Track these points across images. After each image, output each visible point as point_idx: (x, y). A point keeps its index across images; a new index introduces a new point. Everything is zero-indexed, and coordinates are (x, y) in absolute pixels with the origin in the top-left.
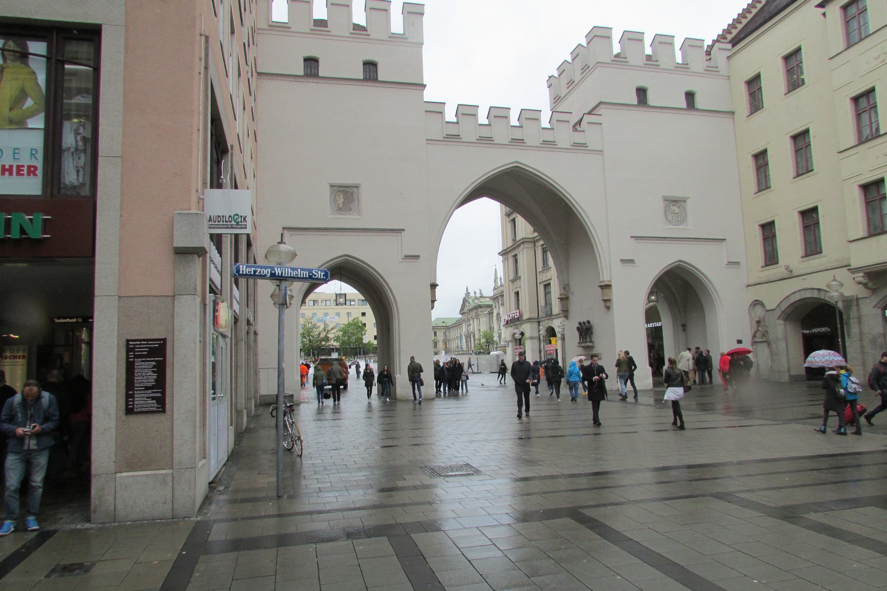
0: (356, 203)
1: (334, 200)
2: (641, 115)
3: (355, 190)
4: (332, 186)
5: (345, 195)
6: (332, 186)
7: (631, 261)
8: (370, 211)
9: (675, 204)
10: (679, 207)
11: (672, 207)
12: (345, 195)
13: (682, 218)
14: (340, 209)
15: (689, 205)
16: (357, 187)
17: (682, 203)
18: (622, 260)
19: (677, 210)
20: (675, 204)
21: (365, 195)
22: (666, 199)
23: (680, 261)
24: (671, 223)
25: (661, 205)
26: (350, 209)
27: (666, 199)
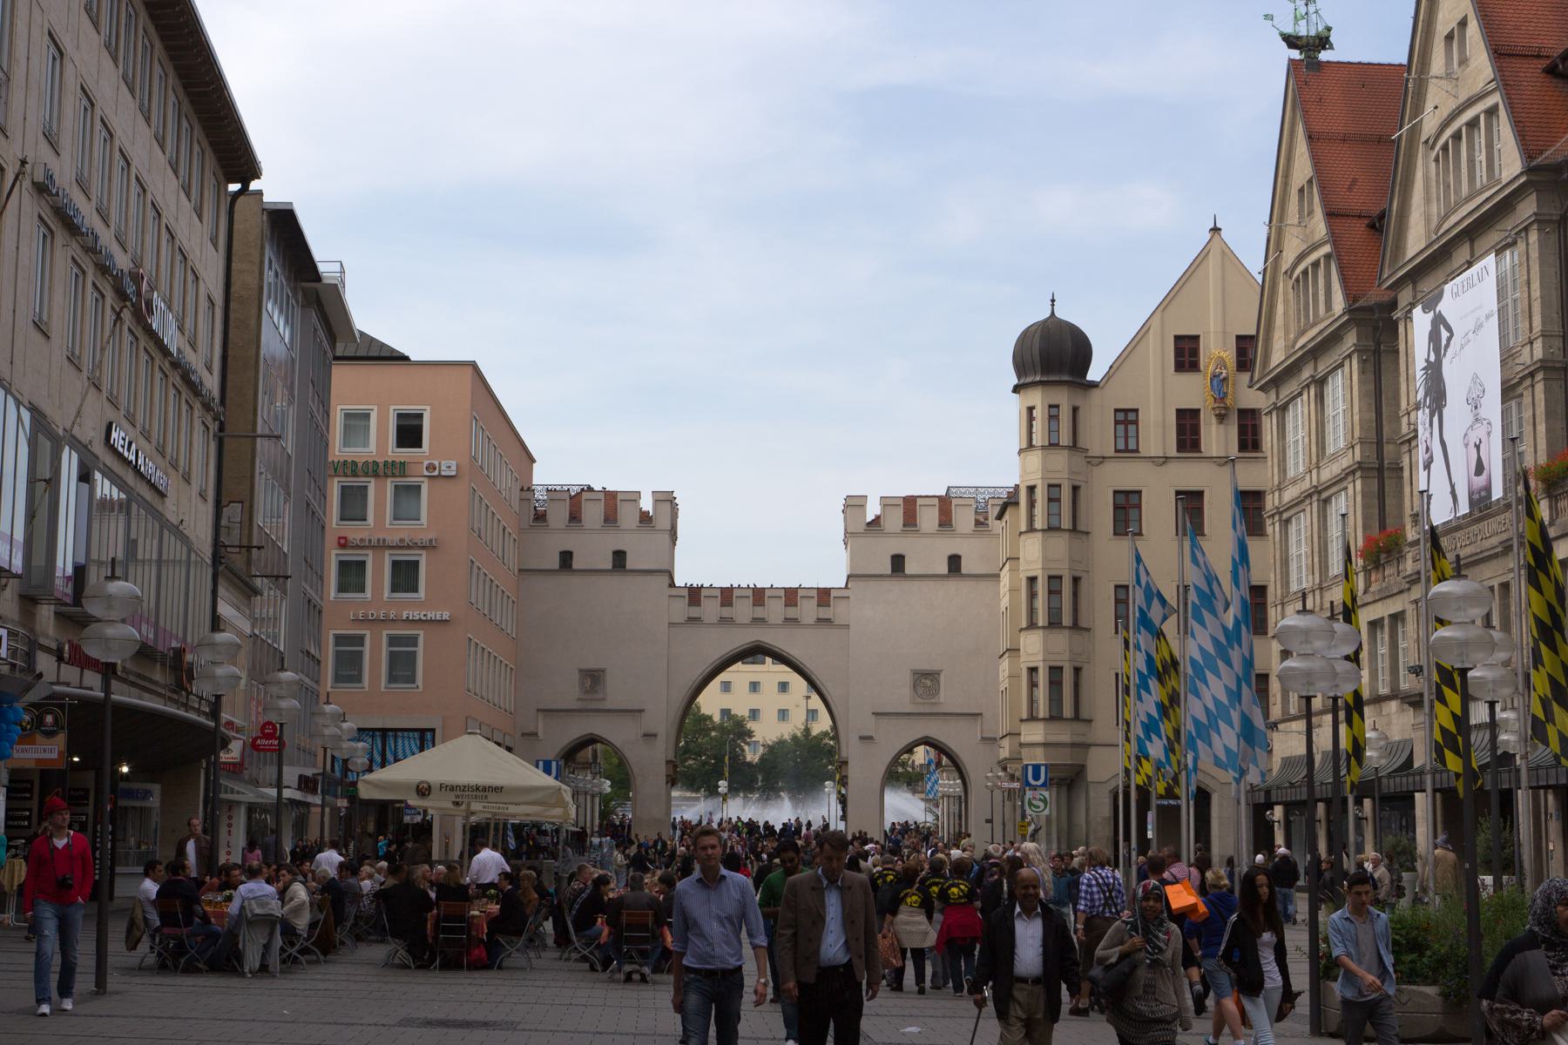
1: (582, 684)
2: (896, 587)
4: (581, 671)
5: (593, 678)
6: (581, 671)
7: (871, 738)
8: (616, 693)
9: (926, 680)
13: (934, 691)
14: (587, 692)
15: (942, 679)
18: (861, 738)
19: (928, 683)
20: (926, 680)
22: (915, 673)
24: (921, 696)
25: (908, 678)
27: (915, 673)
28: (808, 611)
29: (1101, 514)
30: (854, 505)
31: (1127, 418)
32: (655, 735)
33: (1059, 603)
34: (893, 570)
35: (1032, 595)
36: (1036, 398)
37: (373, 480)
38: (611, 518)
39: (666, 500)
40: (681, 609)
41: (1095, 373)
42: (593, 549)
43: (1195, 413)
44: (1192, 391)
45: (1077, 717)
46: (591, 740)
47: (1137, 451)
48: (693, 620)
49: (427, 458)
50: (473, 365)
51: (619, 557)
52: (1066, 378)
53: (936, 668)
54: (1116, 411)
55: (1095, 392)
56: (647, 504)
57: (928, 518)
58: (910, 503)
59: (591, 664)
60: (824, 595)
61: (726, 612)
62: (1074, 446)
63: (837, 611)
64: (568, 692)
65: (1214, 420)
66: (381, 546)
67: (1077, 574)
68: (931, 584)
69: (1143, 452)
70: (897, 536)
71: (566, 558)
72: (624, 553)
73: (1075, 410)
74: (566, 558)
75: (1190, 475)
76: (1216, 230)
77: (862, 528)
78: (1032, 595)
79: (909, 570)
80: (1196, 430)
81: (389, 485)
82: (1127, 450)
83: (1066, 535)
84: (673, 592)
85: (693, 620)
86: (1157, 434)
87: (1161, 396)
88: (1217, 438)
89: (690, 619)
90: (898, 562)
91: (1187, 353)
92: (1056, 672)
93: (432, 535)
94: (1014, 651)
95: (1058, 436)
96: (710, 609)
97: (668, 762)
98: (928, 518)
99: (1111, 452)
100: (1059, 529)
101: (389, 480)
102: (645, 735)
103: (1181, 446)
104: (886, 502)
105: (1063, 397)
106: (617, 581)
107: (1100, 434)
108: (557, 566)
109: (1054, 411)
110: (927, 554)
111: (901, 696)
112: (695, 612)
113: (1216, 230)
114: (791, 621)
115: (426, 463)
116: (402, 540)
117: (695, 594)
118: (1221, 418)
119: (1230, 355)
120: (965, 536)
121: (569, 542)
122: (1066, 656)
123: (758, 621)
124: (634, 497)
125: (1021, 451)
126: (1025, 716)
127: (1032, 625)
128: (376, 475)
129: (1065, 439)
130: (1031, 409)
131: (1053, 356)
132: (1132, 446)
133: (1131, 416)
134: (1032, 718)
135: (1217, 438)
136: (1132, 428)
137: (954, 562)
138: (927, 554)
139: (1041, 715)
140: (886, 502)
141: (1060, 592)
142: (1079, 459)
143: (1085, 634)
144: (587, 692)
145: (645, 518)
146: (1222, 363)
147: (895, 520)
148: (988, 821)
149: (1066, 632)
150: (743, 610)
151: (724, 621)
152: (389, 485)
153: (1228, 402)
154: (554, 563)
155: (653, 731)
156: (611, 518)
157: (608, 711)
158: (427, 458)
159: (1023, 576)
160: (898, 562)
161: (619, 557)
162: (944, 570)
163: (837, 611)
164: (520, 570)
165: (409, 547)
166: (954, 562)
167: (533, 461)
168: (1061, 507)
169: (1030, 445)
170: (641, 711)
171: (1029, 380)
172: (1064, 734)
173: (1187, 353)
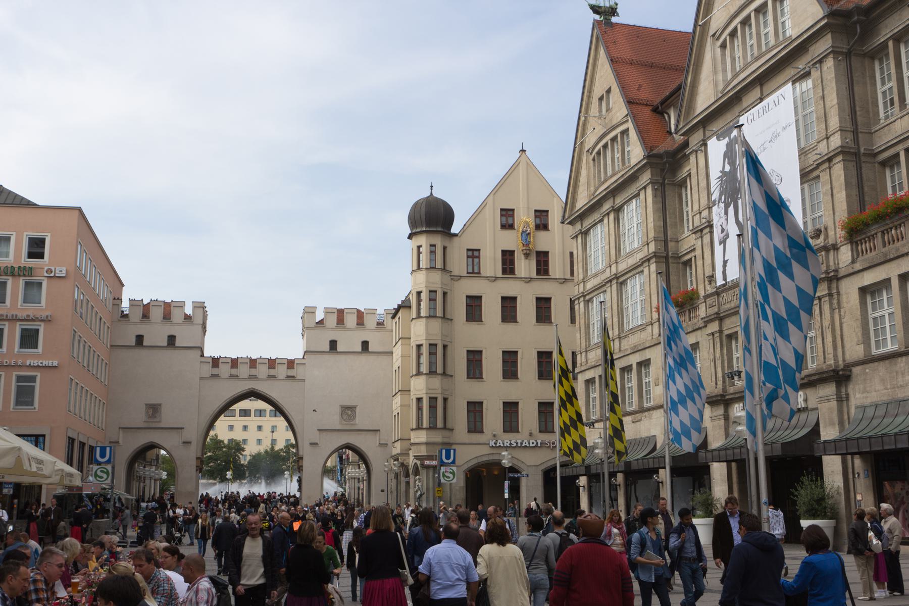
1: (147, 412)
2: (332, 358)
5: (154, 409)
7: (316, 444)
8: (167, 418)
9: (348, 411)
12: (154, 409)
13: (353, 417)
14: (150, 417)
15: (357, 410)
16: (160, 405)
18: (311, 444)
19: (350, 412)
20: (348, 411)
22: (342, 407)
25: (338, 410)
27: (342, 407)
28: (281, 371)
29: (459, 309)
30: (309, 311)
31: (474, 254)
32: (190, 443)
33: (436, 360)
35: (419, 355)
36: (422, 240)
37: (10, 278)
38: (167, 317)
39: (200, 307)
40: (207, 370)
41: (455, 229)
42: (156, 334)
43: (512, 253)
44: (511, 240)
45: (445, 428)
46: (153, 446)
47: (479, 273)
48: (214, 376)
49: (47, 265)
50: (79, 210)
51: (172, 339)
52: (440, 229)
54: (468, 250)
55: (456, 239)
56: (188, 310)
57: (351, 321)
58: (341, 313)
59: (153, 402)
60: (291, 363)
61: (234, 371)
62: (444, 269)
63: (298, 372)
64: (138, 417)
65: (523, 256)
66: (14, 319)
67: (446, 343)
68: (352, 357)
69: (483, 273)
70: (335, 331)
73: (445, 248)
74: (140, 339)
75: (509, 288)
76: (523, 151)
77: (312, 324)
78: (419, 355)
79: (340, 348)
80: (512, 262)
81: (21, 282)
82: (474, 272)
83: (440, 320)
84: (203, 359)
85: (214, 376)
86: (491, 264)
87: (493, 242)
88: (525, 267)
89: (213, 376)
90: (333, 344)
91: (507, 219)
92: (433, 400)
93: (48, 313)
94: (406, 391)
95: (438, 264)
96: (225, 370)
97: (197, 458)
98: (351, 321)
99: (465, 274)
100: (435, 317)
101: (22, 278)
103: (504, 271)
104: (327, 311)
105: (438, 240)
106: (170, 353)
107: (459, 263)
109: (433, 249)
110: (349, 340)
111: (334, 420)
112: (215, 371)
113: (523, 151)
114: (272, 377)
115: (46, 268)
116: (28, 316)
117: (215, 362)
118: (527, 256)
119: (531, 220)
121: (142, 330)
122: (439, 391)
123: (252, 377)
124: (181, 305)
125: (413, 271)
126: (414, 427)
127: (419, 373)
128: (13, 275)
129: (439, 264)
130: (419, 247)
131: (432, 218)
132: (476, 271)
133: (476, 254)
134: (419, 427)
135: (525, 267)
136: (476, 260)
137: (365, 345)
138: (349, 340)
139: (424, 426)
140: (327, 311)
141: (436, 354)
142: (447, 277)
143: (450, 378)
144: (150, 417)
145: (188, 318)
146: (527, 224)
147: (332, 321)
148: (383, 491)
149: (440, 377)
150: (244, 371)
151: (233, 377)
152: (21, 282)
153: (531, 247)
155: (189, 440)
156: (167, 317)
158: (47, 265)
159: (413, 344)
160: (333, 344)
161: (172, 339)
162: (359, 349)
163: (298, 372)
164: (111, 346)
165: (32, 320)
166: (365, 345)
167: (123, 285)
168: (436, 304)
169: (419, 268)
170: (182, 428)
171: (418, 230)
172: (437, 437)
173: (507, 219)
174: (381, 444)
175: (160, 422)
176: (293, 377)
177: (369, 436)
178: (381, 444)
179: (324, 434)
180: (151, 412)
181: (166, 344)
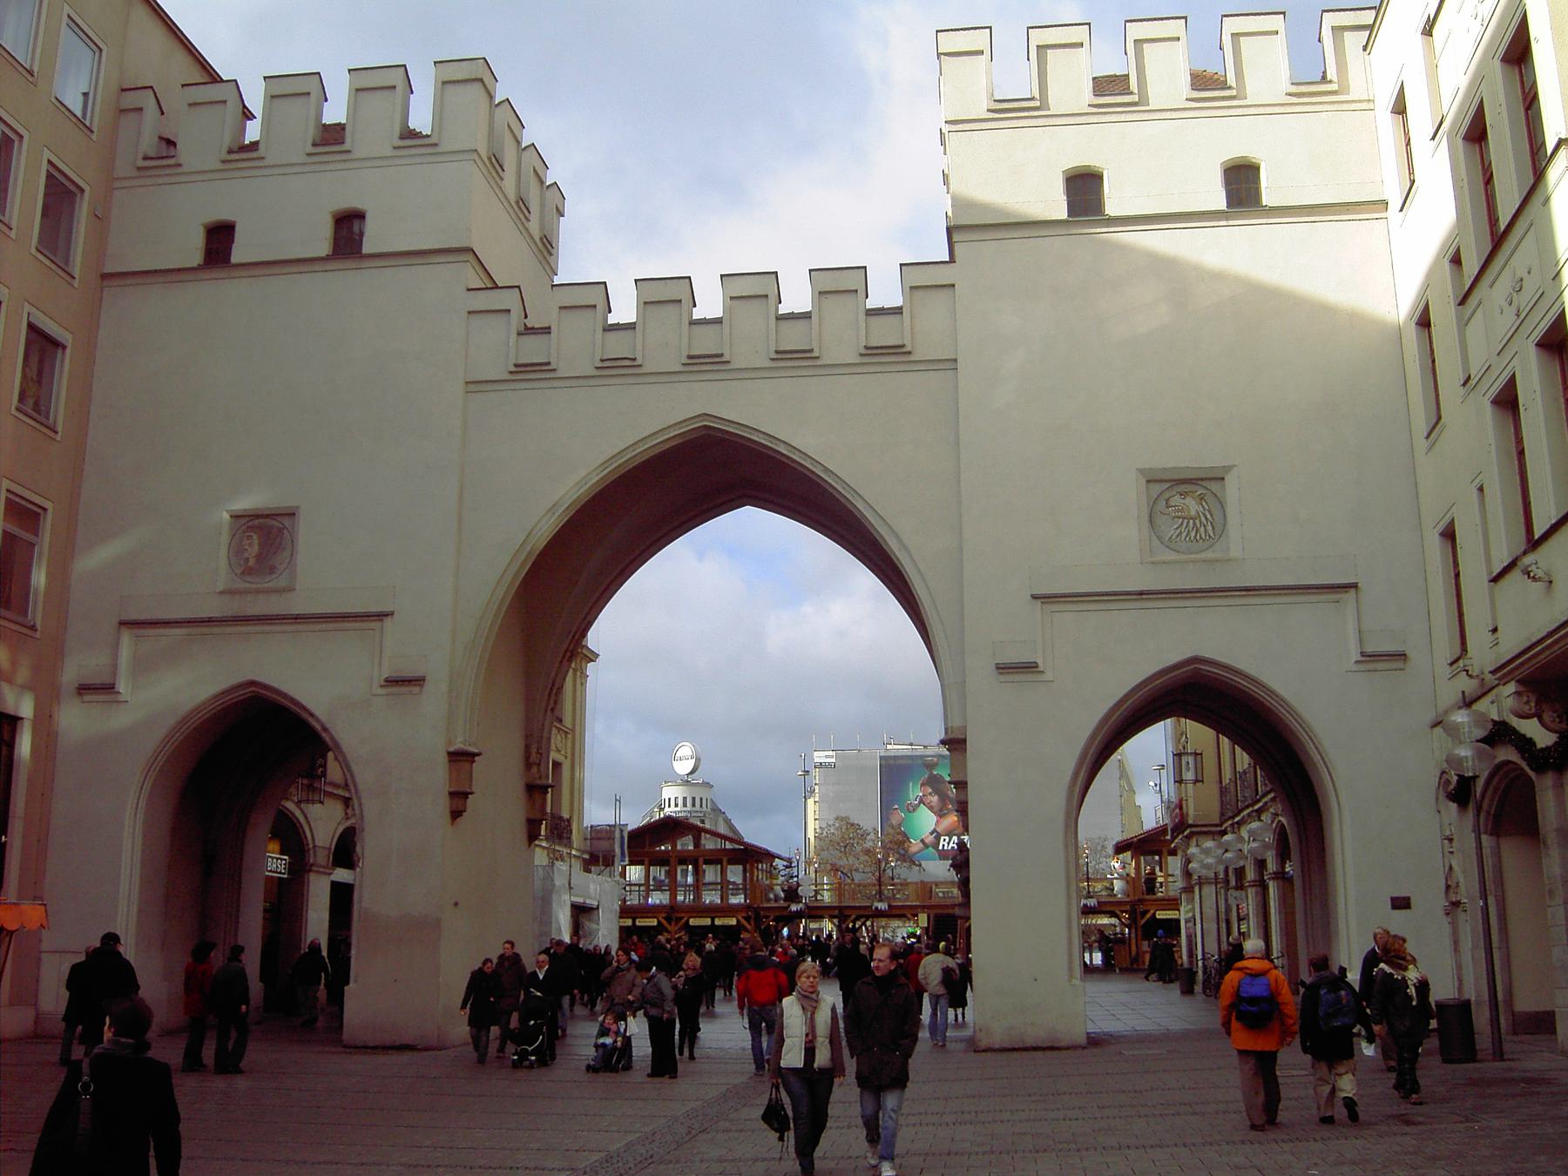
0: (287, 554)
1: (237, 551)
3: (287, 521)
5: (266, 536)
7: (1030, 667)
8: (320, 572)
10: (1202, 498)
11: (1176, 500)
13: (1208, 528)
14: (248, 571)
16: (292, 514)
17: (1214, 486)
18: (1003, 668)
19: (1192, 506)
20: (1185, 495)
21: (307, 535)
22: (1152, 479)
23: (1196, 660)
24: (1169, 545)
25: (1132, 493)
26: (272, 569)
27: (1152, 479)
32: (417, 681)
34: (1072, 210)
48: (524, 370)
51: (348, 226)
53: (1207, 460)
64: (202, 573)
71: (220, 238)
72: (359, 216)
74: (220, 238)
89: (522, 368)
102: (392, 682)
108: (197, 258)
120: (1266, 109)
154: (192, 250)
157: (297, 618)
161: (348, 226)
170: (391, 614)
174: (1368, 657)
175: (291, 589)
176: (897, 350)
177: (1304, 615)
178: (1369, 657)
179: (1067, 618)
180: (253, 548)
181: (324, 249)
